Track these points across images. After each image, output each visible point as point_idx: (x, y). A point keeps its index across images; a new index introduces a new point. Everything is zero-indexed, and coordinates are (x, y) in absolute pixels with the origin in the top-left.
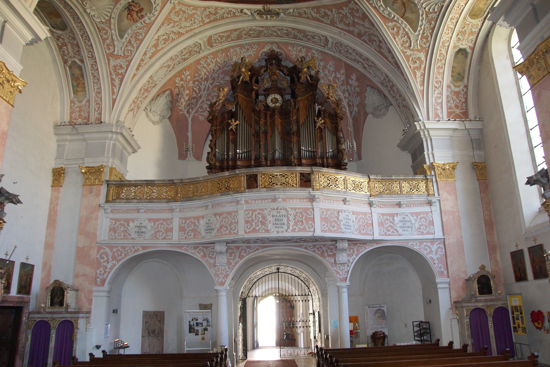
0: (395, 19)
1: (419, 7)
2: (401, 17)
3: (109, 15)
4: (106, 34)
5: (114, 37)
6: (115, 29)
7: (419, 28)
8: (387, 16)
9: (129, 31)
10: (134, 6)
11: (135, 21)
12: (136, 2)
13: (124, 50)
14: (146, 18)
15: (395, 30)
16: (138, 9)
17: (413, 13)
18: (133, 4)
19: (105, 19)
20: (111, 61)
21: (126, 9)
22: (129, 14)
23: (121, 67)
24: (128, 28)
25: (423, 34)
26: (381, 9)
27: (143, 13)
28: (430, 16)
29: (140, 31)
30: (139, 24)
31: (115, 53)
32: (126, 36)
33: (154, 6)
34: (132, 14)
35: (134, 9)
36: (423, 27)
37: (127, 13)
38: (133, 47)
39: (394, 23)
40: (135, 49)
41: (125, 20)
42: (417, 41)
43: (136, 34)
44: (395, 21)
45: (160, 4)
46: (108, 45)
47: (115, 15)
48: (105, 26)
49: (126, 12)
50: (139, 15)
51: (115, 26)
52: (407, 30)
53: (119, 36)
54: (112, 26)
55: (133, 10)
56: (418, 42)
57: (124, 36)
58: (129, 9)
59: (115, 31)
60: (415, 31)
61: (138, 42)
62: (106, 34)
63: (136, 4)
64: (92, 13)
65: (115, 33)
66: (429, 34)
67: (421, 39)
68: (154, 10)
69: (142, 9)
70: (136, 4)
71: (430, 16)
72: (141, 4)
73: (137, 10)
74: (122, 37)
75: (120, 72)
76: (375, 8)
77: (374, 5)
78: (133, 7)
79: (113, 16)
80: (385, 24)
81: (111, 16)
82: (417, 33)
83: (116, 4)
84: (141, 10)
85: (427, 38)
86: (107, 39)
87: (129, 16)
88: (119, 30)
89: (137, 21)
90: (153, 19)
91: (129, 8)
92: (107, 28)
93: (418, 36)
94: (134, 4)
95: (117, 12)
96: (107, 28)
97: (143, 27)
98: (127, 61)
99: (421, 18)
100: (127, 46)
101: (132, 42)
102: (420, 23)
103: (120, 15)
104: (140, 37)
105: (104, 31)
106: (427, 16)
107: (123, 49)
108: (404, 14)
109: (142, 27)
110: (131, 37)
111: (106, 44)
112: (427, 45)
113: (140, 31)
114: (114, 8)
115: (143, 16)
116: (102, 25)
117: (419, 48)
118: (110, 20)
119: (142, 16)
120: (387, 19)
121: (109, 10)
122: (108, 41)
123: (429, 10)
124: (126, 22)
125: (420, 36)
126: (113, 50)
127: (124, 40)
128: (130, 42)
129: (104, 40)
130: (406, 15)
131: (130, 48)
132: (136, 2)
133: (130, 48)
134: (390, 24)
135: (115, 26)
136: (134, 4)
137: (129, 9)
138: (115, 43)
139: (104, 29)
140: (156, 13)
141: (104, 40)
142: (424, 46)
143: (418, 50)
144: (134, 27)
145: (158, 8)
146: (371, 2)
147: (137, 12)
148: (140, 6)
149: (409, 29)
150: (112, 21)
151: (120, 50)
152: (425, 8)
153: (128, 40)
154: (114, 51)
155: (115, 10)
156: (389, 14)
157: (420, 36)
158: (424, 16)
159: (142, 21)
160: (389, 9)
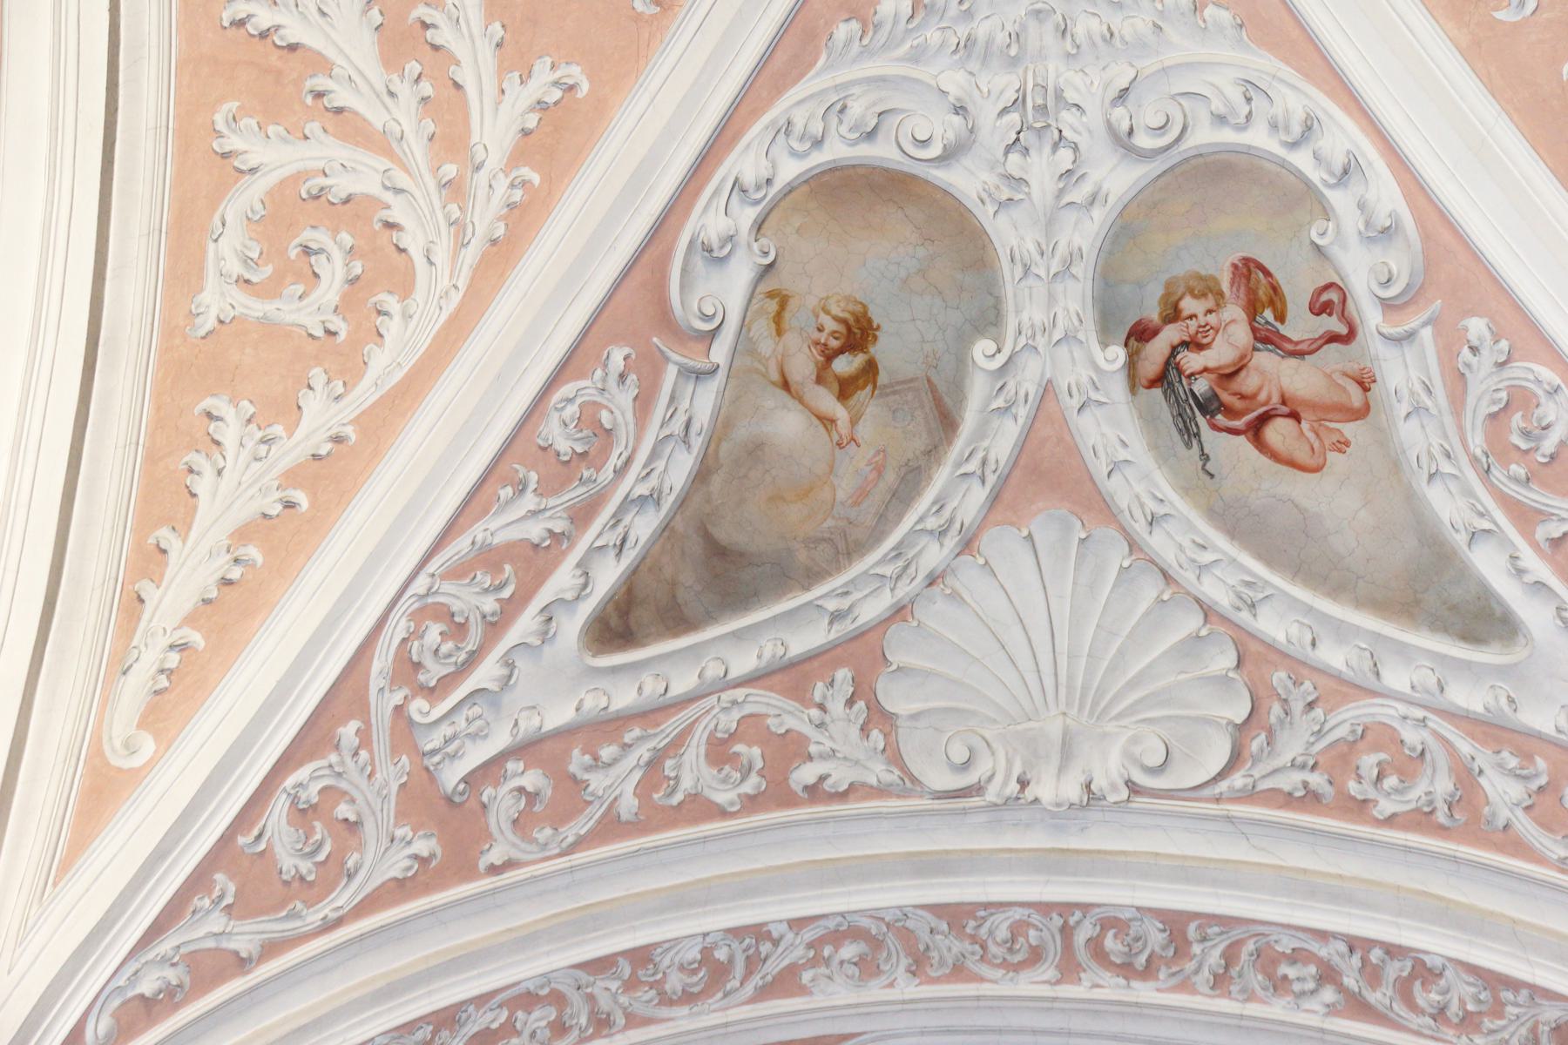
4: (1410, 764)
5: (1469, 697)
9: (1447, 507)
11: (1360, 398)
12: (1153, 314)
14: (1360, 272)
16: (1234, 312)
18: (1156, 351)
19: (1223, 680)
21: (1189, 434)
22: (1255, 431)
24: (1411, 498)
27: (1298, 289)
29: (1485, 388)
30: (1401, 373)
32: (1488, 564)
33: (1259, 138)
34: (1269, 396)
35: (1219, 354)
37: (1242, 443)
43: (1499, 449)
45: (1263, 64)
47: (1225, 570)
48: (1304, 726)
49: (1230, 450)
50: (1300, 325)
53: (1470, 637)
54: (1334, 656)
55: (1228, 376)
57: (1486, 594)
58: (1210, 405)
62: (1410, 764)
63: (1173, 314)
64: (1108, 769)
65: (1414, 668)
68: (1302, 160)
69: (1248, 270)
70: (1173, 314)
72: (1187, 265)
73: (1241, 334)
74: (1483, 621)
78: (1191, 361)
79: (1222, 598)
81: (1208, 612)
84: (1257, 287)
86: (1466, 777)
87: (1279, 432)
90: (1387, 196)
91: (1198, 402)
92: (1347, 718)
94: (1171, 334)
95: (1185, 535)
97: (1451, 344)
103: (1239, 522)
105: (1369, 762)
109: (1448, 353)
110: (1526, 518)
111: (1526, 827)
113: (1485, 388)
114: (1133, 546)
115: (1330, 300)
116: (1292, 746)
118: (1252, 654)
119: (1320, 308)
122: (1503, 792)
124: (1334, 499)
127: (1534, 615)
129: (1465, 815)
132: (1153, 314)
135: (1342, 632)
136: (1171, 334)
137: (1210, 405)
139: (1342, 757)
140: (1342, 136)
144: (1414, 437)
145: (1296, 97)
147: (1266, 338)
148: (1206, 288)
150: (1273, 626)
153: (1539, 568)
155: (1160, 543)
159: (1371, 317)
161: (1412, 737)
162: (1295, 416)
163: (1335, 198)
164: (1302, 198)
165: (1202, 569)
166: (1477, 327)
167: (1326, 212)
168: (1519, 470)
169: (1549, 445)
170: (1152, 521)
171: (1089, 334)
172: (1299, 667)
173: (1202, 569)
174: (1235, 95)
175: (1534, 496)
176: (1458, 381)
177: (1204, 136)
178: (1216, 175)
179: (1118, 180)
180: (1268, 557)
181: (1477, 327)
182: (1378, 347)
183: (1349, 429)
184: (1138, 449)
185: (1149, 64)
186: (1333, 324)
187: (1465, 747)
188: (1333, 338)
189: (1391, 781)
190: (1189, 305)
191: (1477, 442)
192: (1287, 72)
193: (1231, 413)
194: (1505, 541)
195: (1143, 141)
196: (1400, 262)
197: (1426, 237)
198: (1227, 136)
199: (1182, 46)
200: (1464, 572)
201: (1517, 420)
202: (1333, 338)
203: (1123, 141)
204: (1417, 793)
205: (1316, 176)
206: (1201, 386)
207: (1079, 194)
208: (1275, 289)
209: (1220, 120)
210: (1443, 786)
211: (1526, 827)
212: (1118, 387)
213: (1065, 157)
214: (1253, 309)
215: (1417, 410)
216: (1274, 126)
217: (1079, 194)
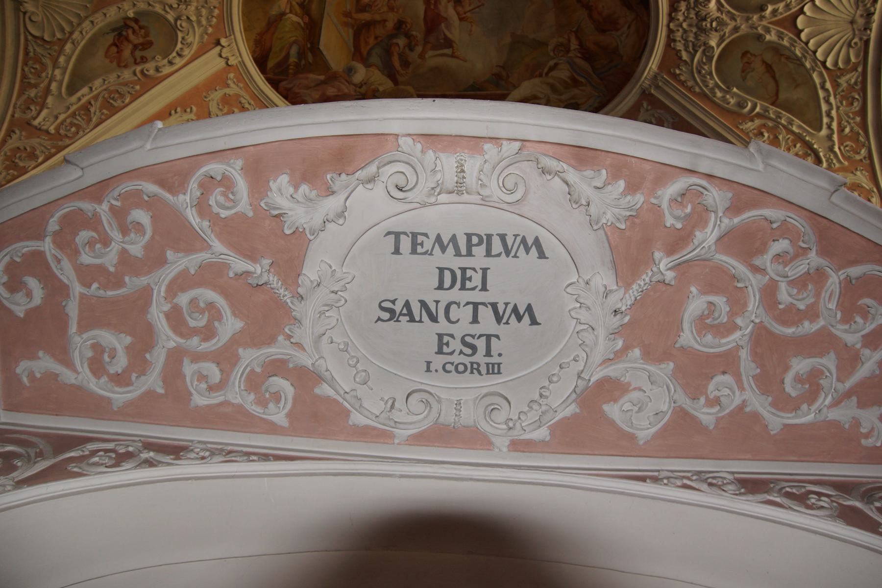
0: (758, 110)
1: (808, 65)
2: (772, 104)
3: (67, 29)
5: (54, 86)
6: (66, 68)
7: (825, 120)
8: (736, 109)
9: (97, 83)
10: (134, 32)
11: (122, 65)
13: (62, 123)
14: (150, 67)
15: (766, 135)
16: (141, 40)
17: (797, 86)
18: (133, 24)
20: (14, 136)
21: (113, 30)
22: (114, 44)
23: (33, 156)
25: (841, 129)
26: (719, 94)
27: (146, 53)
28: (843, 81)
30: (127, 74)
31: (36, 123)
32: (85, 90)
33: (179, 46)
35: (132, 37)
36: (834, 113)
37: (111, 41)
38: (90, 120)
39: (758, 122)
40: (91, 126)
41: (101, 53)
42: (831, 149)
43: (111, 92)
44: (759, 115)
45: (195, 47)
46: (32, 100)
49: (110, 39)
50: (138, 54)
51: (68, 62)
52: (794, 129)
54: (62, 59)
55: (127, 39)
56: (836, 149)
58: (120, 35)
59: (64, 74)
60: (820, 129)
61: (105, 111)
63: (141, 28)
65: (61, 76)
66: (856, 128)
67: (841, 143)
68: (174, 54)
69: (151, 43)
70: (141, 28)
71: (843, 81)
73: (136, 42)
74: (72, 89)
75: (21, 164)
76: (703, 95)
77: (697, 90)
78: (130, 32)
80: (738, 128)
81: (71, 33)
82: (824, 132)
83: (95, 12)
85: (854, 136)
86: (36, 86)
87: (114, 49)
88: (75, 74)
89: (126, 66)
90: (167, 70)
91: (121, 32)
92: (48, 62)
93: (830, 137)
94: (136, 27)
95: (88, 30)
96: (48, 62)
97: (134, 83)
98: (53, 147)
99: (821, 94)
100: (74, 115)
101: (92, 110)
102: (824, 107)
103: (93, 41)
104: (118, 103)
106: (836, 85)
107: (62, 117)
108: (777, 94)
109: (132, 82)
110: (96, 98)
111: (24, 97)
112: (863, 152)
114: (86, 17)
115: (144, 60)
117: (846, 163)
118: (62, 42)
119: (142, 58)
120: (739, 115)
121: (75, 20)
122: (33, 93)
123: (836, 64)
125: (835, 137)
126: (34, 113)
127: (74, 99)
128: (86, 109)
129: (26, 85)
130: (783, 96)
131: (79, 120)
132: (142, 23)
133: (79, 120)
134: (749, 126)
136: (136, 27)
137: (120, 35)
138: (50, 100)
141: (26, 85)
142: (858, 157)
143: (843, 169)
144: (112, 78)
145: (188, 53)
146: (690, 84)
147: (135, 47)
148: (147, 35)
149: (800, 127)
150: (68, 47)
151: (52, 120)
152: (824, 63)
153: (84, 100)
154: (35, 118)
156: (741, 105)
157: (835, 137)
158: (828, 85)
159: (138, 69)
160: (735, 90)
161: (44, 75)
162: (118, 52)
163: (166, 61)
164: (166, 55)
165: (81, 32)
166: (138, 87)
167: (164, 58)
168: (106, 96)
169: (111, 101)
170: (92, 22)
171: (135, 9)
172: (60, 52)
173: (81, 32)
174: (189, 41)
175: (100, 99)
176: (126, 84)
177: (180, 35)
178: (173, 39)
179: (170, 17)
180: (85, 47)
181: (138, 87)
182: (133, 69)
183: (115, 64)
184: (109, 19)
185: (195, 25)
186: (139, 60)
187: (42, 85)
188: (135, 60)
189: (33, 71)
190: (143, 31)
191: (112, 88)
192: (193, 52)
193: (118, 39)
194: (89, 94)
195: (179, 23)
196: (152, 72)
197: (157, 78)
198: (180, 39)
199: (198, 31)
200: (83, 86)
201: (117, 95)
202: (135, 60)
203: (178, 18)
204: (30, 76)
205: (170, 57)
206: (124, 33)
207: (167, 8)
208: (146, 49)
209: (183, 38)
210: (33, 81)
211: (24, 97)
212: (122, 15)
213: (175, 6)
214: (142, 44)
215: (119, 77)
216: (181, 49)
217: (167, 8)
